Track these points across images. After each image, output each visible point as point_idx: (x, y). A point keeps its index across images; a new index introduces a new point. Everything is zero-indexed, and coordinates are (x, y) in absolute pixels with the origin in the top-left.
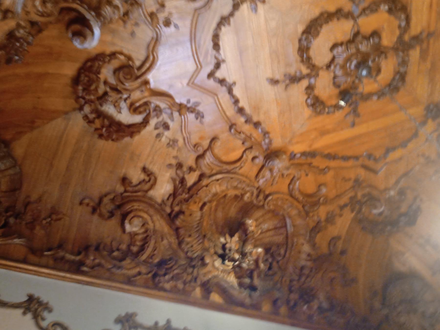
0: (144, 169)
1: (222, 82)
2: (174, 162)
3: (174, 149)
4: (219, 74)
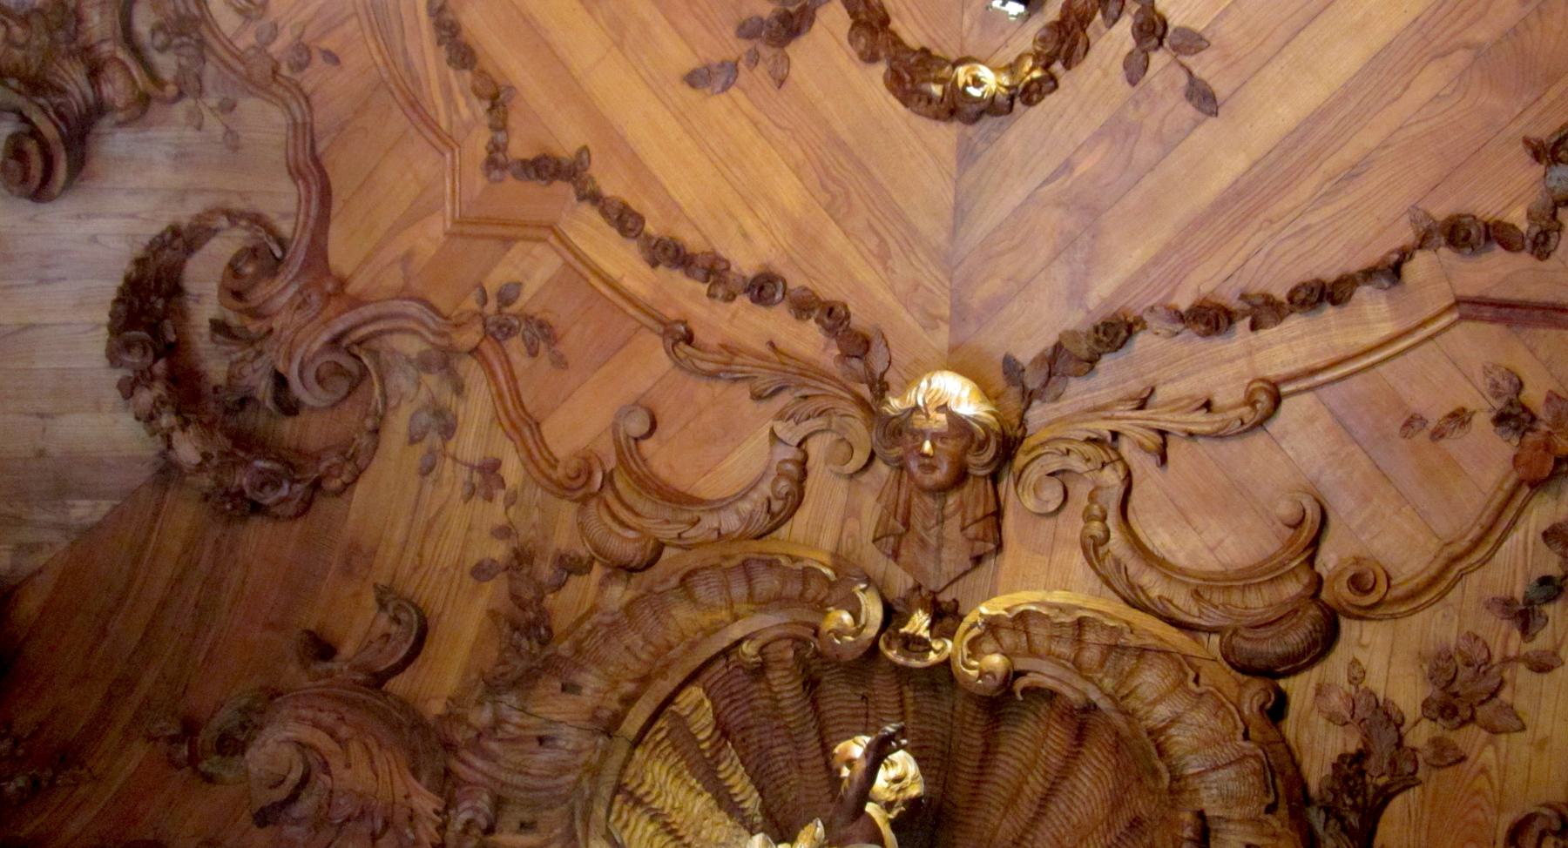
0: (384, 597)
1: (545, 168)
2: (499, 551)
3: (490, 498)
4: (519, 148)
